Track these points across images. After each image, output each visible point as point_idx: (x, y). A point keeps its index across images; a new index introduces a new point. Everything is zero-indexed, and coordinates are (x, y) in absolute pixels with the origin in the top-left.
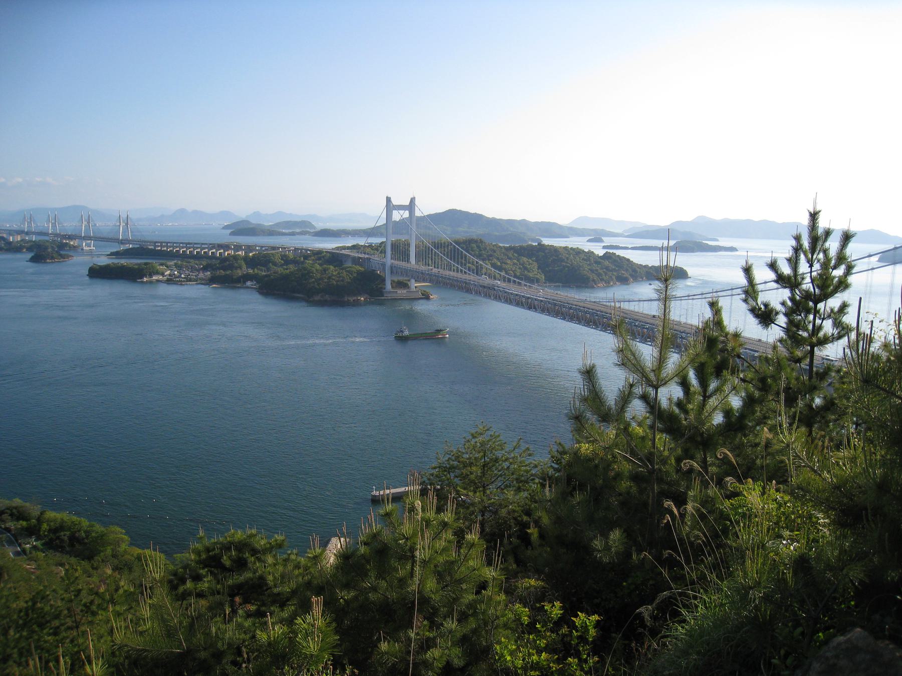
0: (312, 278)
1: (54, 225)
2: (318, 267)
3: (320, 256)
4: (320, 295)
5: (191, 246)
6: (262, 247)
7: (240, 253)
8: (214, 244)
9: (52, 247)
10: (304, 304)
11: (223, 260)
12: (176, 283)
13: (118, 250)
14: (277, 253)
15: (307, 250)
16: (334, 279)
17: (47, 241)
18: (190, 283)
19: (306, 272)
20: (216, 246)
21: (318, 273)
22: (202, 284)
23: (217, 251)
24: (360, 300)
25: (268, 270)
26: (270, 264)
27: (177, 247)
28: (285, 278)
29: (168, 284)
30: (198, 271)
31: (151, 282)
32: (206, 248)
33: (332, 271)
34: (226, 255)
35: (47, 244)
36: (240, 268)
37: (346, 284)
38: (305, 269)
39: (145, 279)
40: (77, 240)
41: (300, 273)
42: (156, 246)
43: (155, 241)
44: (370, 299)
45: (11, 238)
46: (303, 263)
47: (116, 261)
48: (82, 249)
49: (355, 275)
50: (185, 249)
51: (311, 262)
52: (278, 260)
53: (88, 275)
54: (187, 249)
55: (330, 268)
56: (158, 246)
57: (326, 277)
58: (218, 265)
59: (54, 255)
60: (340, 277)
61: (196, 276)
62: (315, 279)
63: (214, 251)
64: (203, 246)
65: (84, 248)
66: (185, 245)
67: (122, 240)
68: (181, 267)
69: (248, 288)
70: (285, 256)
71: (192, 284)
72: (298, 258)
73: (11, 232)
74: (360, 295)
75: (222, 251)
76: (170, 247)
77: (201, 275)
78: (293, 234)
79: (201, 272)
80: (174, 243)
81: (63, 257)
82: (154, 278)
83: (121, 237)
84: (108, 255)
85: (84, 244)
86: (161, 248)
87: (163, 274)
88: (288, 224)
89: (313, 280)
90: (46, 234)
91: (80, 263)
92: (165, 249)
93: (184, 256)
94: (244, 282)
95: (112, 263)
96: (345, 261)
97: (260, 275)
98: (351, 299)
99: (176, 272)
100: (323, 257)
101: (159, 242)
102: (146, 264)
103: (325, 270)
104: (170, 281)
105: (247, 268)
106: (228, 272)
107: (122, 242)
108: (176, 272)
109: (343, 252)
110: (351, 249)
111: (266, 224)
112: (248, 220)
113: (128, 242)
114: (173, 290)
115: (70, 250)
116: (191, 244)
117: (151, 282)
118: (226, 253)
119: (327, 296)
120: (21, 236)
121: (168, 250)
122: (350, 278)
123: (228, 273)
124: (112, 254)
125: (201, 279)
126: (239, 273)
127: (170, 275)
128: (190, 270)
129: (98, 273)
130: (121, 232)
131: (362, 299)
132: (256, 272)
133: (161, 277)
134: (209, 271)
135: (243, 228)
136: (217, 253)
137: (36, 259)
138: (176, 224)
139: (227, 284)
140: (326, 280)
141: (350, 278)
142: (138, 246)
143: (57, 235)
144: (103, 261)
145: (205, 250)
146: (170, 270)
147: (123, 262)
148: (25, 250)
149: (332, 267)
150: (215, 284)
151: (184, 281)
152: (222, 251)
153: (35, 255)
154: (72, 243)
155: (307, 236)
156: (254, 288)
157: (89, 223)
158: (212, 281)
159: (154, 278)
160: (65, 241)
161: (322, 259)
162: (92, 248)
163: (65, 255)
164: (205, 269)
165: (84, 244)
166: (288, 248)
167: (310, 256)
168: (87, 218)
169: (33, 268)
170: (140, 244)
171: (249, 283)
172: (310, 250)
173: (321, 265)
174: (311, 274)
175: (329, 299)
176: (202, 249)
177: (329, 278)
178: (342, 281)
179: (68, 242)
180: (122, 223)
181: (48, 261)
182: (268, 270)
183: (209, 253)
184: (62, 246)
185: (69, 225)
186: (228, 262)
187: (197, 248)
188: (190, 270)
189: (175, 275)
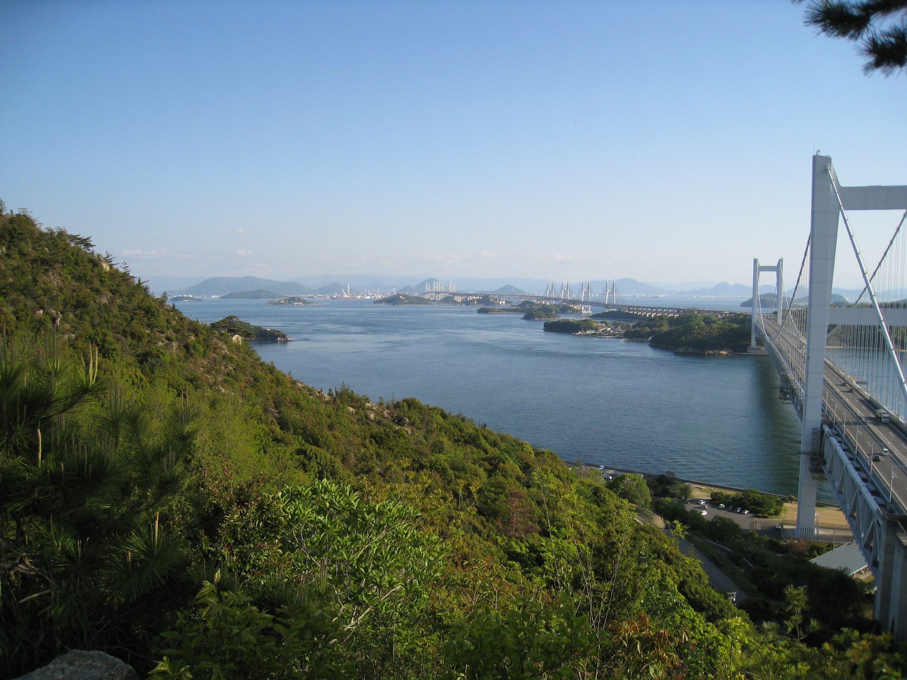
1: (566, 292)
73: (538, 298)
85: (583, 308)
113: (613, 306)
143: (564, 300)
154: (575, 307)
162: (590, 312)
165: (583, 308)
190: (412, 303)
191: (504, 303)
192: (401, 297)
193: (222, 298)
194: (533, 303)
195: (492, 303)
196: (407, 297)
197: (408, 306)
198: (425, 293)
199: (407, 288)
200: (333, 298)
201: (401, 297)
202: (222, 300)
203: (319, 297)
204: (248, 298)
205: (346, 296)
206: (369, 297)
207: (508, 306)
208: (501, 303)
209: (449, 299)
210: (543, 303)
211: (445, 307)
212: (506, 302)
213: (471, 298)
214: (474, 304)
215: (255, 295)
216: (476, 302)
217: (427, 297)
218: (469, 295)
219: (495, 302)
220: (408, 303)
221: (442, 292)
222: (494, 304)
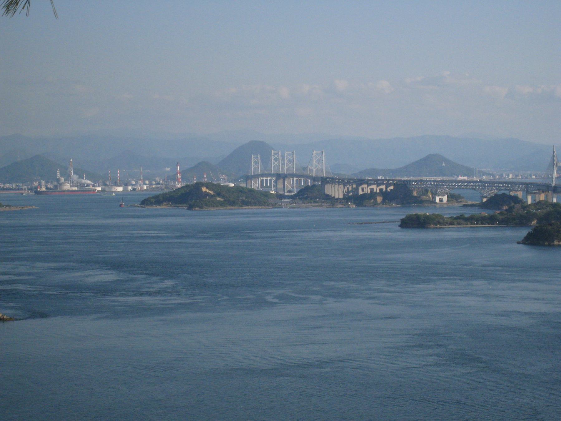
73: (529, 188)
190: (233, 203)
191: (445, 198)
192: (204, 189)
194: (516, 199)
195: (419, 202)
196: (220, 190)
197: (222, 210)
198: (248, 178)
199: (202, 167)
200: (38, 193)
201: (204, 189)
207: (456, 210)
208: (437, 199)
210: (542, 197)
212: (452, 197)
214: (375, 204)
216: (379, 199)
217: (255, 185)
218: (361, 182)
219: (425, 198)
220: (222, 204)
221: (293, 176)
222: (421, 202)
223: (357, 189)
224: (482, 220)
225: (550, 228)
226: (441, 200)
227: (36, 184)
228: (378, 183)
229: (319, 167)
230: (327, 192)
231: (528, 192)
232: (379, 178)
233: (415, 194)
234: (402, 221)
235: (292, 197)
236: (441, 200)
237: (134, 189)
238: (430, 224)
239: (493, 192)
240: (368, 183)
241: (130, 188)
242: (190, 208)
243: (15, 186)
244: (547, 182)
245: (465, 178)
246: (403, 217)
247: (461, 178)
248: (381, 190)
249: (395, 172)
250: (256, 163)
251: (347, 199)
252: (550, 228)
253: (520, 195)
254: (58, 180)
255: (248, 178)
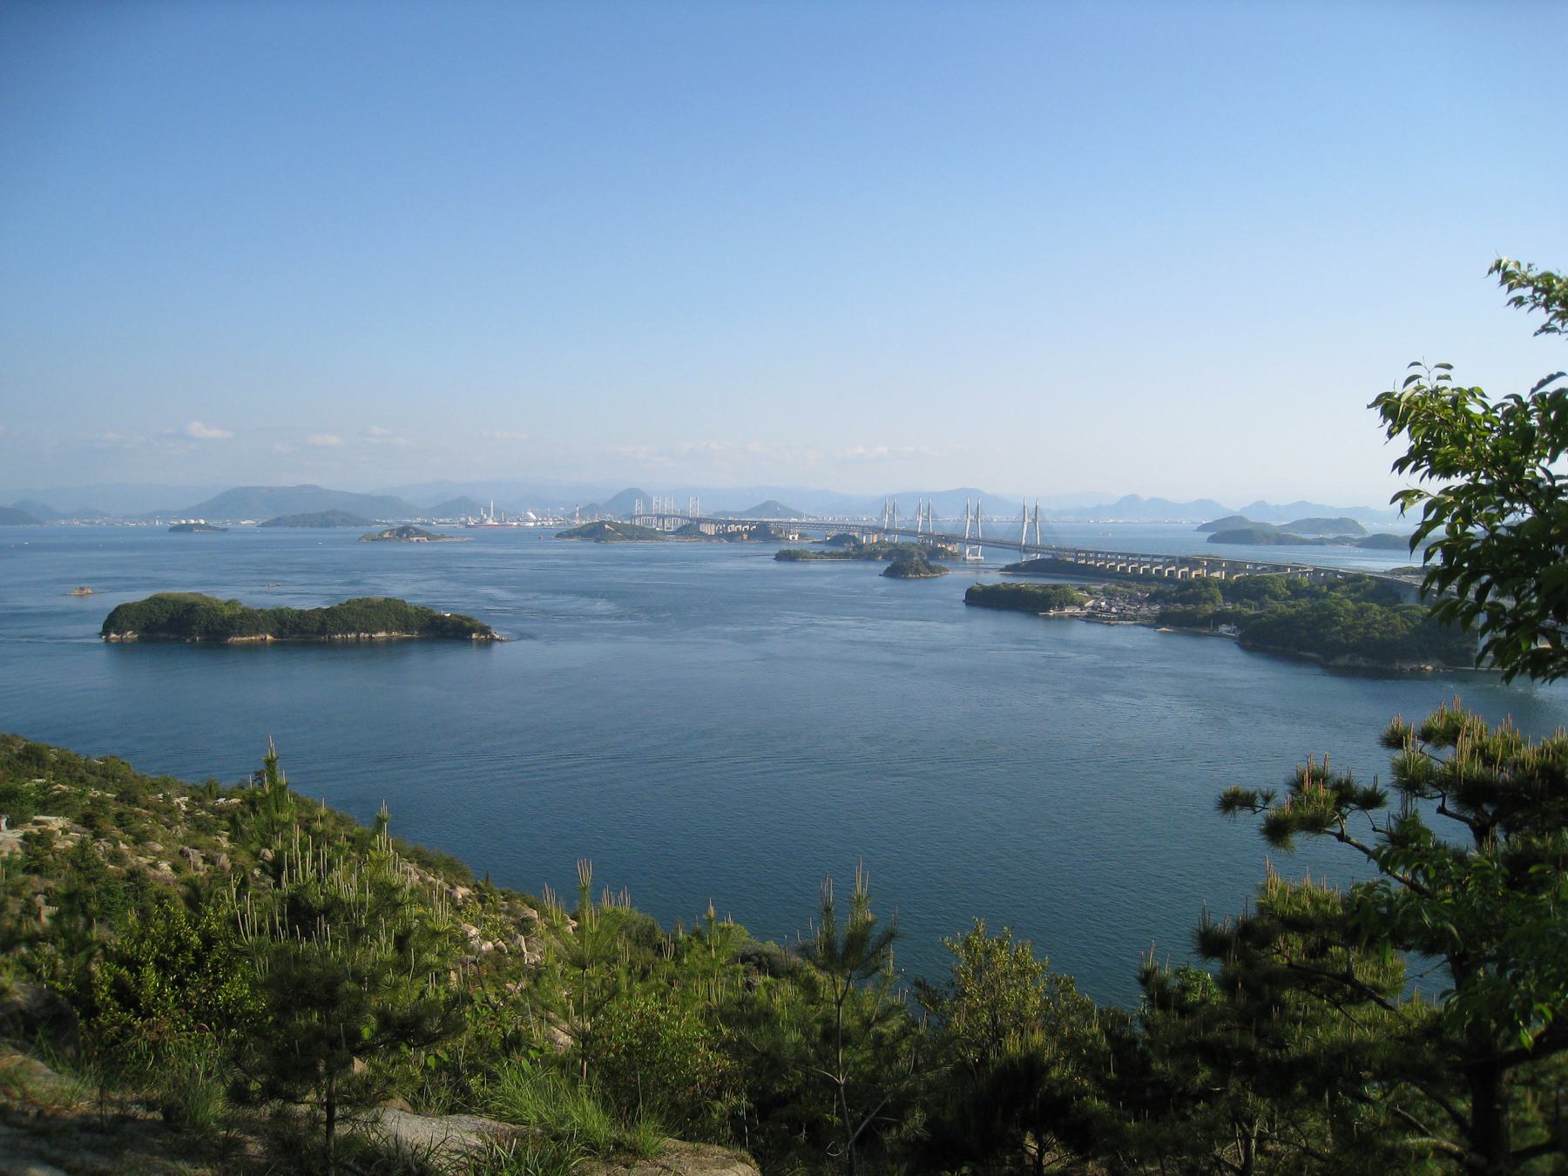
0: (1337, 625)
2: (1350, 605)
3: (1358, 584)
4: (1348, 656)
5: (1137, 559)
6: (1256, 565)
7: (1217, 574)
8: (1175, 557)
9: (920, 554)
10: (1318, 671)
11: (1186, 584)
12: (1101, 621)
13: (1019, 561)
14: (1280, 577)
15: (1337, 573)
16: (1377, 629)
17: (914, 544)
18: (1124, 622)
19: (1327, 613)
20: (1177, 561)
21: (1348, 615)
22: (1143, 625)
23: (1177, 570)
24: (1424, 669)
25: (1262, 606)
26: (1267, 596)
27: (1111, 560)
28: (1286, 622)
29: (1087, 621)
30: (1141, 603)
31: (1061, 618)
32: (1161, 563)
33: (1375, 614)
34: (1193, 576)
35: (913, 549)
36: (1213, 599)
37: (1399, 638)
38: (1324, 607)
39: (1052, 613)
40: (958, 544)
41: (1315, 614)
42: (1077, 558)
43: (1078, 549)
44: (1444, 669)
45: (865, 538)
46: (1325, 596)
47: (1009, 580)
48: (965, 559)
49: (1419, 622)
50: (1125, 565)
51: (1339, 595)
52: (1282, 590)
53: (964, 601)
54: (1128, 565)
55: (1371, 608)
56: (1082, 558)
57: (1363, 623)
58: (1174, 594)
59: (920, 568)
60: (1389, 624)
61: (1136, 611)
62: (1342, 627)
63: (1173, 568)
64: (1155, 560)
65: (968, 558)
66: (1125, 558)
67: (1025, 546)
68: (1113, 595)
69: (1221, 636)
70: (1294, 582)
71: (1126, 625)
72: (1317, 587)
74: (1425, 659)
75: (1187, 569)
76: (1101, 560)
77: (1145, 610)
78: (1321, 542)
79: (1145, 604)
80: (1109, 553)
81: (931, 570)
82: (1066, 611)
83: (1024, 542)
84: (1001, 570)
85: (968, 551)
86: (1086, 562)
87: (1081, 605)
88: (1314, 524)
89: (1339, 628)
90: (914, 534)
91: (957, 581)
92: (1093, 562)
93: (1123, 577)
94: (1216, 626)
95: (1004, 583)
96: (1405, 596)
97: (1245, 615)
98: (1407, 667)
99: (1103, 604)
100: (1364, 586)
101: (1083, 552)
102: (1055, 587)
103: (1362, 611)
104: (1090, 618)
105: (1224, 603)
106: (1190, 608)
107: (1025, 549)
108: (1103, 604)
109: (1403, 578)
110: (1419, 574)
111: (1275, 523)
112: (1244, 516)
113: (1036, 549)
114: (1096, 632)
115: (946, 559)
116: (1134, 555)
117: (1061, 618)
118: (1194, 573)
119: (1361, 658)
120: (878, 537)
121: (1098, 565)
122: (1408, 627)
123: (1190, 608)
124: (1008, 568)
125: (1145, 617)
126: (1209, 609)
127: (1093, 607)
128: (1127, 601)
129: (982, 599)
130: (1025, 533)
131: (1429, 668)
132: (1238, 609)
133: (1078, 610)
134: (1159, 604)
135: (1233, 531)
136: (1177, 572)
137: (892, 573)
138: (1121, 521)
139: (1185, 628)
140: (1362, 630)
141: (1408, 627)
142: (1050, 557)
143: (929, 536)
144: (993, 579)
145: (1157, 568)
146: (1094, 598)
147: (1023, 582)
148: (880, 558)
149: (1376, 607)
150: (1164, 625)
151: (1114, 619)
152: (1187, 569)
153: (893, 565)
154: (950, 549)
155: (1347, 547)
156: (1231, 637)
157: (977, 517)
158: (1160, 620)
159: (1066, 611)
160: (939, 546)
161: (1362, 590)
162: (979, 557)
163: (935, 567)
164: (1153, 599)
165: (968, 551)
166: (1302, 568)
167: (1340, 584)
168: (974, 510)
169: (886, 585)
170: (1052, 554)
171: (1223, 629)
172: (1341, 574)
173: (1355, 601)
174: (1335, 618)
175: (1364, 664)
176: (1155, 564)
177: (1367, 627)
178: (1392, 632)
179: (944, 546)
180: (1026, 520)
181: (910, 576)
182: (1262, 606)
183: (1164, 573)
184: (935, 553)
185: (948, 520)
186: (1191, 590)
187: (1145, 563)
188: (1127, 601)
189: (1101, 607)
193: (263, 525)
195: (776, 539)
202: (265, 529)
203: (440, 524)
204: (311, 526)
205: (490, 522)
206: (532, 524)
208: (791, 537)
209: (689, 529)
211: (686, 547)
213: (733, 528)
215: (326, 520)
216: (745, 536)
219: (780, 535)
222: (778, 539)
223: (727, 528)
224: (831, 555)
225: (905, 564)
226: (793, 538)
227: (463, 519)
228: (744, 523)
229: (669, 508)
230: (701, 530)
231: (863, 533)
232: (730, 519)
233: (773, 532)
234: (776, 554)
235: (673, 533)
236: (793, 538)
237: (543, 525)
238: (798, 557)
239: (834, 533)
240: (736, 523)
241: (539, 523)
242: (597, 541)
243: (448, 520)
244: (880, 525)
245: (796, 520)
246: (777, 552)
247: (793, 520)
248: (746, 529)
249: (749, 512)
250: (639, 505)
251: (718, 536)
252: (905, 564)
253: (856, 534)
254: (482, 516)
255: (633, 517)
